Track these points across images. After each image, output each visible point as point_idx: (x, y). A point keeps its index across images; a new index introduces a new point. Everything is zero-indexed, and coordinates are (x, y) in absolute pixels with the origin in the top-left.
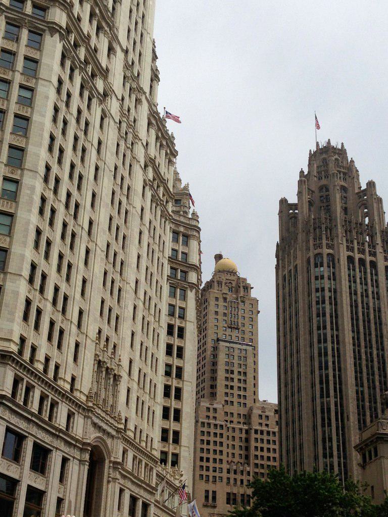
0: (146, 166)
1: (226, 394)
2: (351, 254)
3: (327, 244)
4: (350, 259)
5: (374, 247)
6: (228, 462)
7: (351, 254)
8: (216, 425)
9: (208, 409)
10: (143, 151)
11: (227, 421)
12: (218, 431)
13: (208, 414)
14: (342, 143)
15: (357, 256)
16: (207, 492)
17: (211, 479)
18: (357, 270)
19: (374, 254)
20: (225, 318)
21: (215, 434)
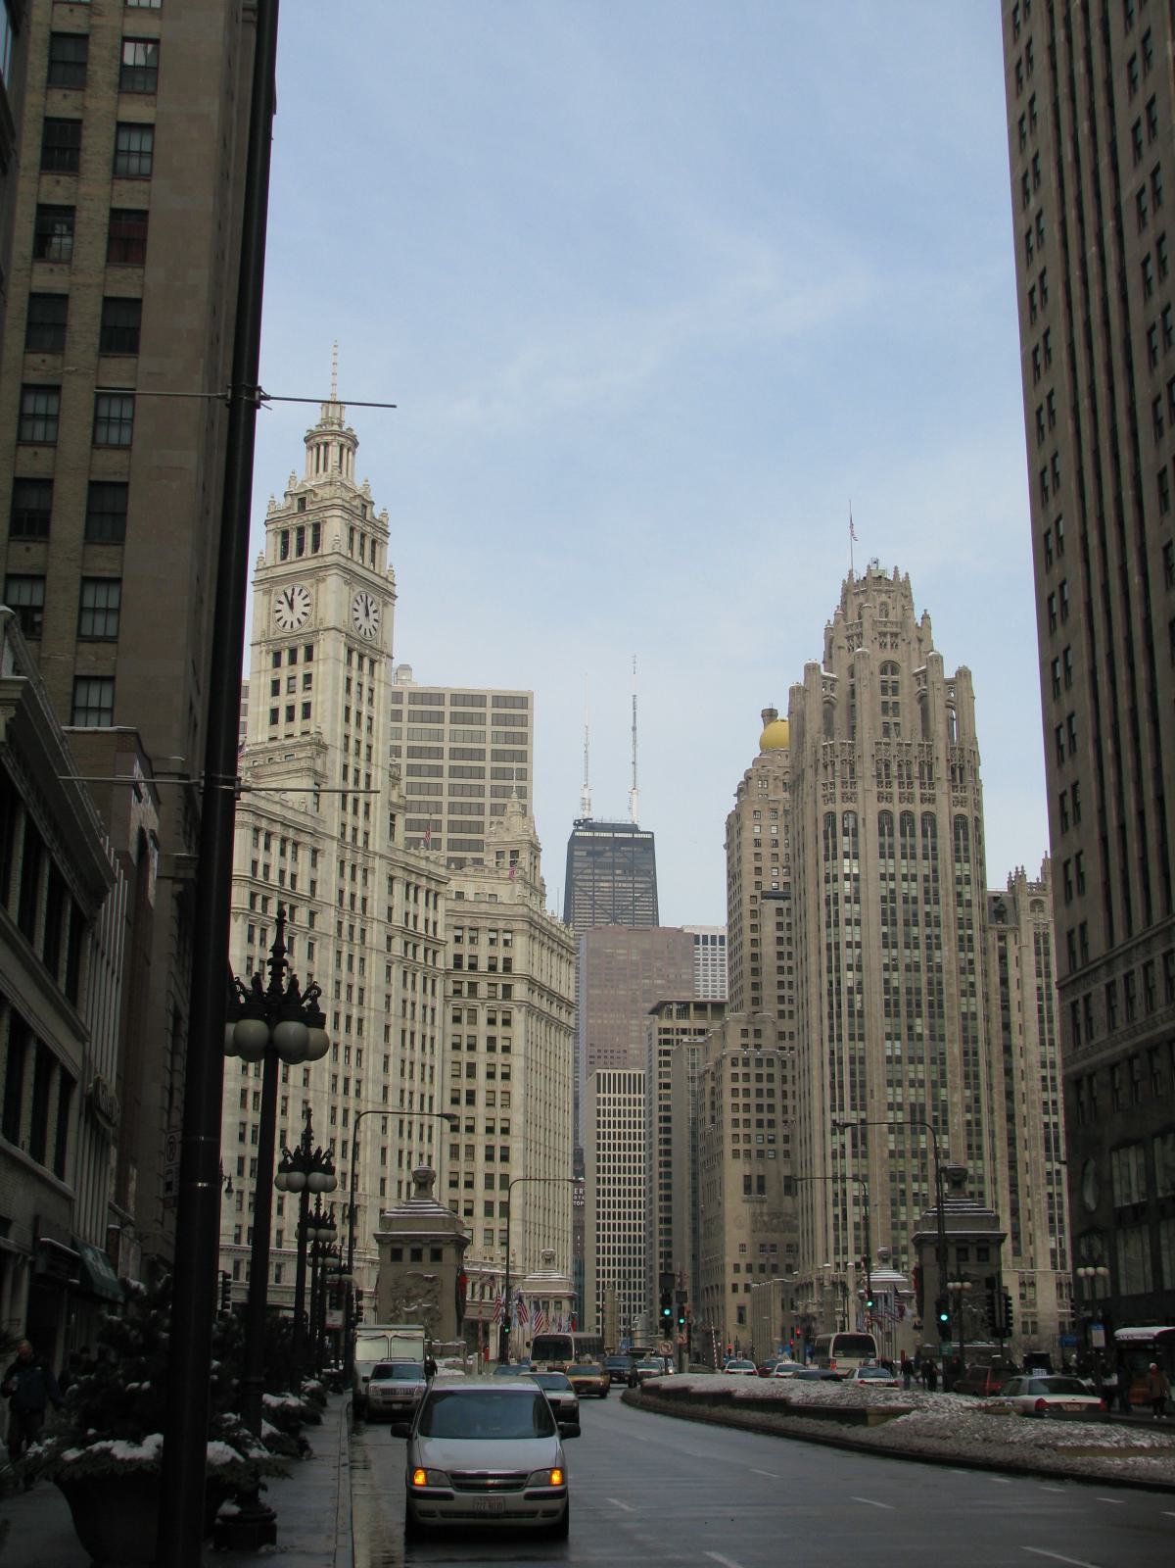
0: (389, 939)
1: (781, 999)
2: (885, 806)
3: (844, 794)
4: (885, 817)
5: (932, 785)
6: (785, 1122)
7: (885, 806)
8: (759, 1062)
9: (745, 1033)
10: (382, 927)
11: (782, 1048)
12: (765, 1070)
13: (745, 1041)
14: (896, 568)
15: (896, 809)
16: (747, 1178)
17: (754, 1154)
18: (897, 834)
19: (932, 800)
20: (775, 851)
21: (759, 1077)
